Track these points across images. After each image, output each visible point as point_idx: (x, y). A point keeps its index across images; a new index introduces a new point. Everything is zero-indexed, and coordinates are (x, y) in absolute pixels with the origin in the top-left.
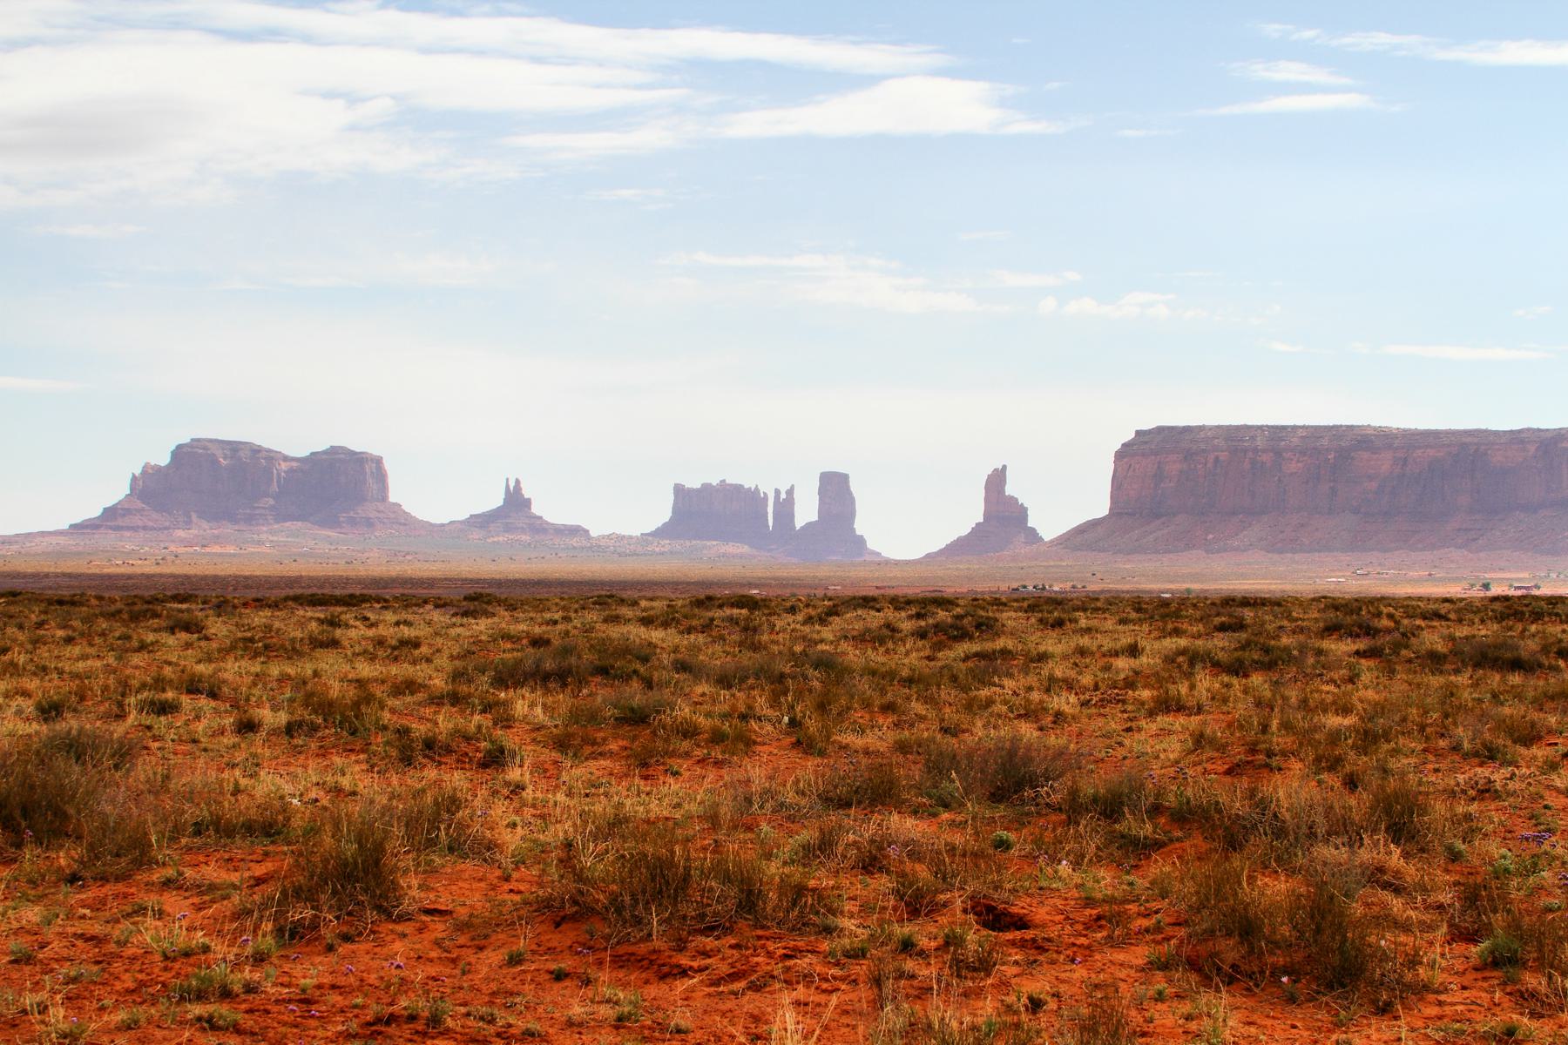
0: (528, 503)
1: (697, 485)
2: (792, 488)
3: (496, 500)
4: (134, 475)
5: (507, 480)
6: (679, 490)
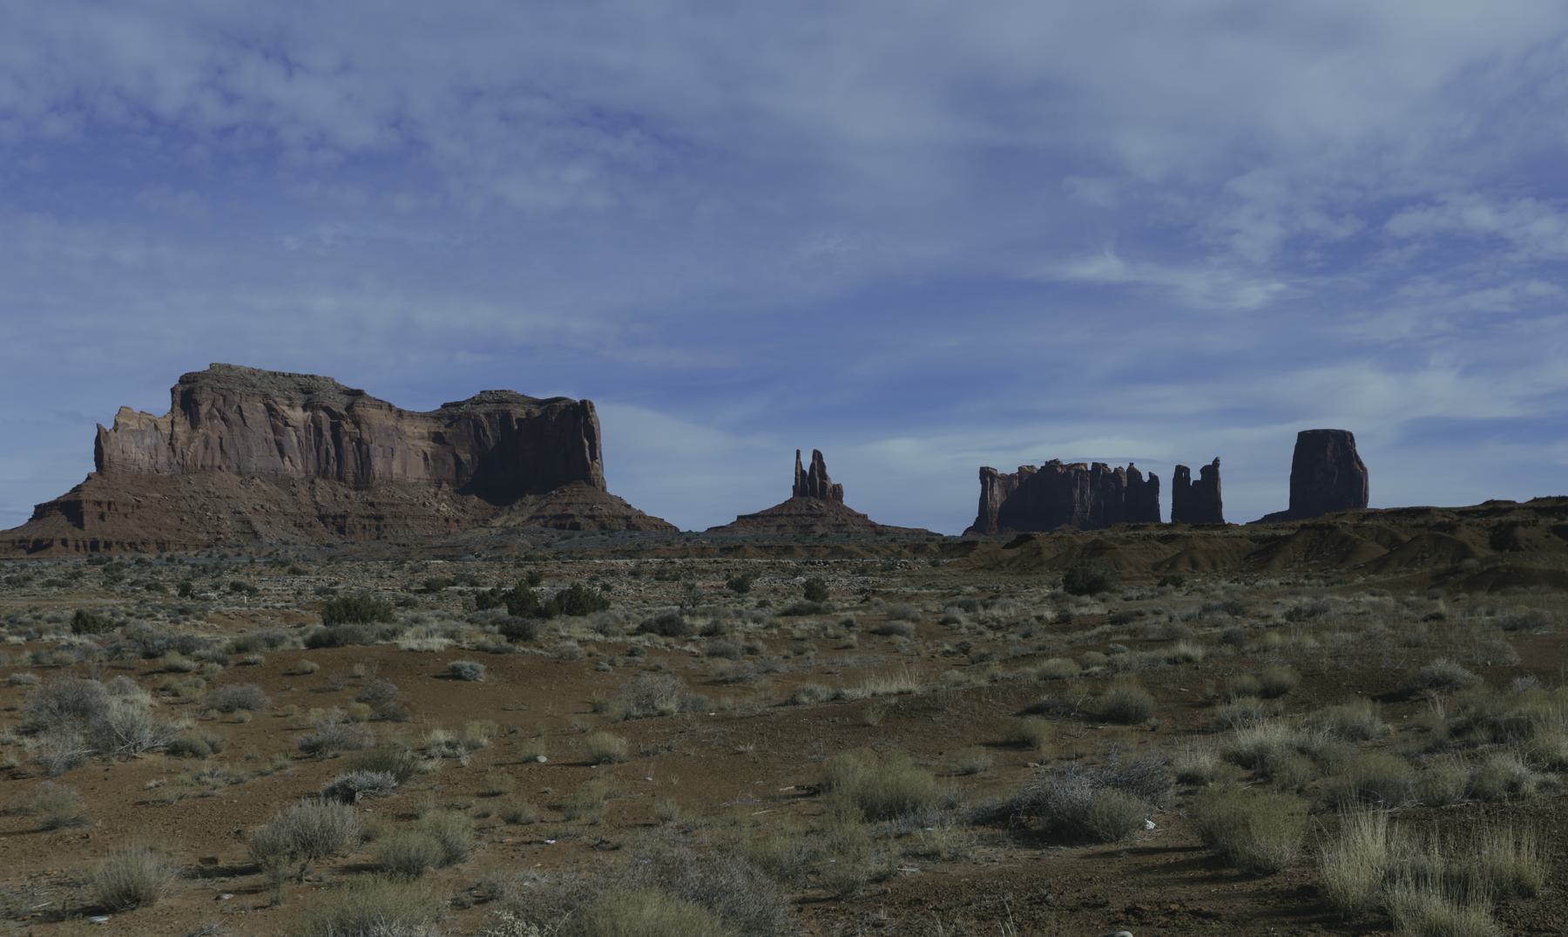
0: (837, 491)
2: (1216, 462)
4: (99, 427)
5: (798, 452)
6: (986, 475)
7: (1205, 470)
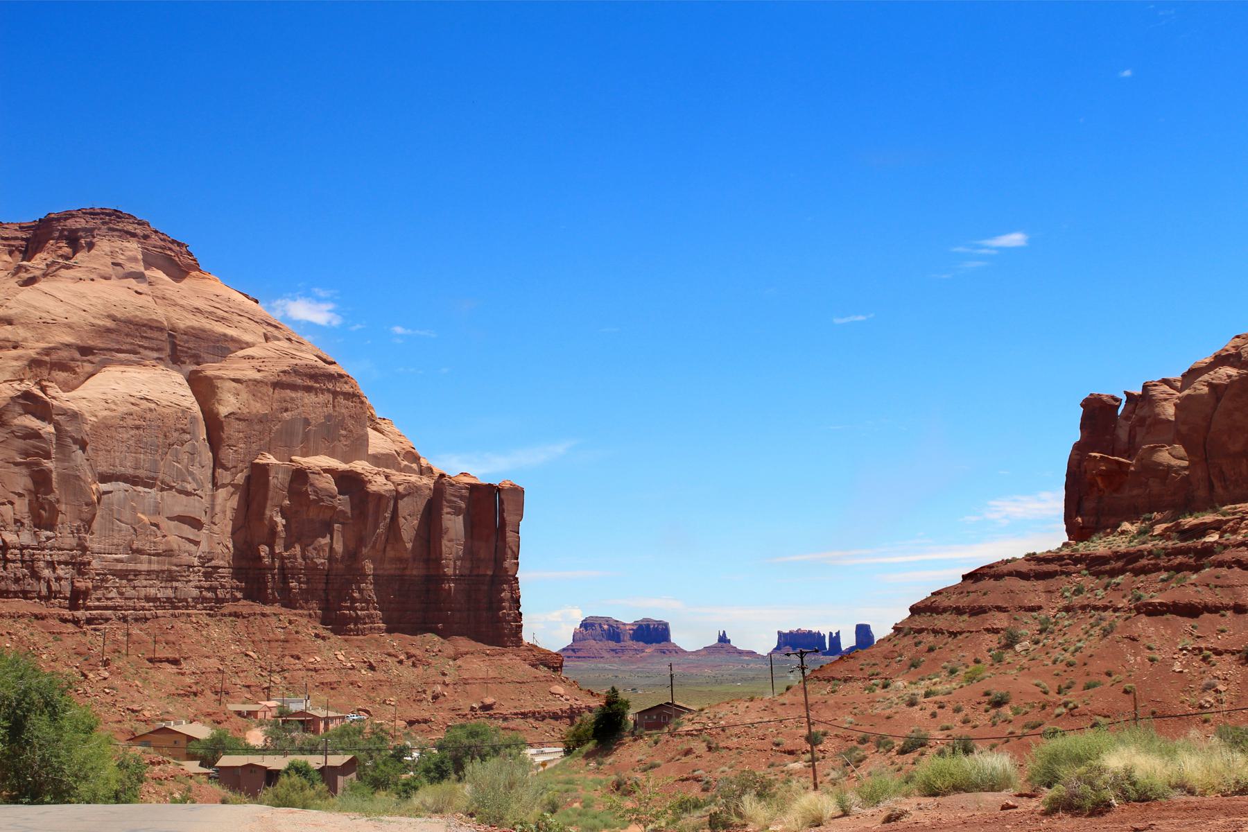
0: (729, 641)
1: (787, 631)
2: (839, 631)
6: (779, 633)
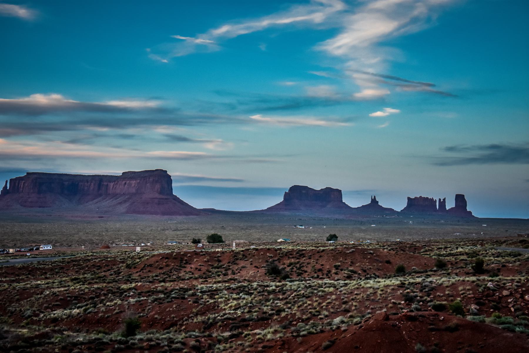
2: (445, 198)
3: (369, 202)
6: (409, 199)
7: (443, 199)
